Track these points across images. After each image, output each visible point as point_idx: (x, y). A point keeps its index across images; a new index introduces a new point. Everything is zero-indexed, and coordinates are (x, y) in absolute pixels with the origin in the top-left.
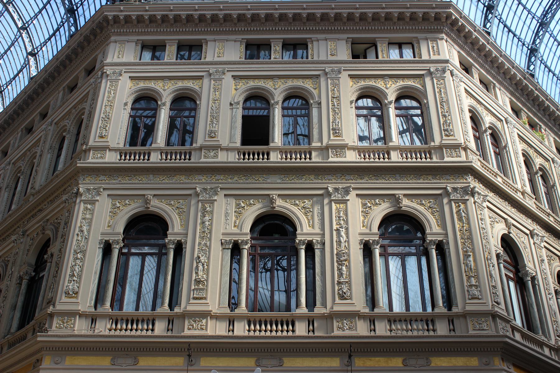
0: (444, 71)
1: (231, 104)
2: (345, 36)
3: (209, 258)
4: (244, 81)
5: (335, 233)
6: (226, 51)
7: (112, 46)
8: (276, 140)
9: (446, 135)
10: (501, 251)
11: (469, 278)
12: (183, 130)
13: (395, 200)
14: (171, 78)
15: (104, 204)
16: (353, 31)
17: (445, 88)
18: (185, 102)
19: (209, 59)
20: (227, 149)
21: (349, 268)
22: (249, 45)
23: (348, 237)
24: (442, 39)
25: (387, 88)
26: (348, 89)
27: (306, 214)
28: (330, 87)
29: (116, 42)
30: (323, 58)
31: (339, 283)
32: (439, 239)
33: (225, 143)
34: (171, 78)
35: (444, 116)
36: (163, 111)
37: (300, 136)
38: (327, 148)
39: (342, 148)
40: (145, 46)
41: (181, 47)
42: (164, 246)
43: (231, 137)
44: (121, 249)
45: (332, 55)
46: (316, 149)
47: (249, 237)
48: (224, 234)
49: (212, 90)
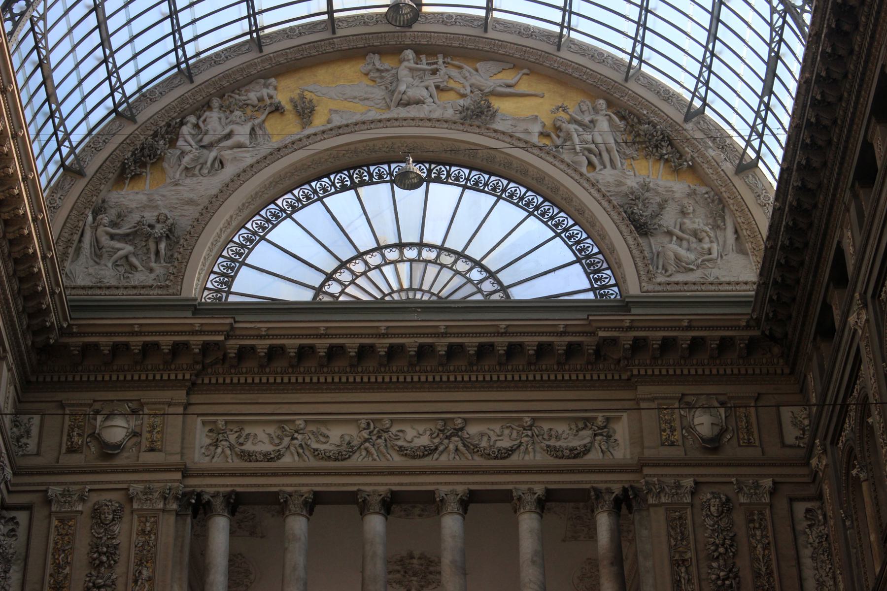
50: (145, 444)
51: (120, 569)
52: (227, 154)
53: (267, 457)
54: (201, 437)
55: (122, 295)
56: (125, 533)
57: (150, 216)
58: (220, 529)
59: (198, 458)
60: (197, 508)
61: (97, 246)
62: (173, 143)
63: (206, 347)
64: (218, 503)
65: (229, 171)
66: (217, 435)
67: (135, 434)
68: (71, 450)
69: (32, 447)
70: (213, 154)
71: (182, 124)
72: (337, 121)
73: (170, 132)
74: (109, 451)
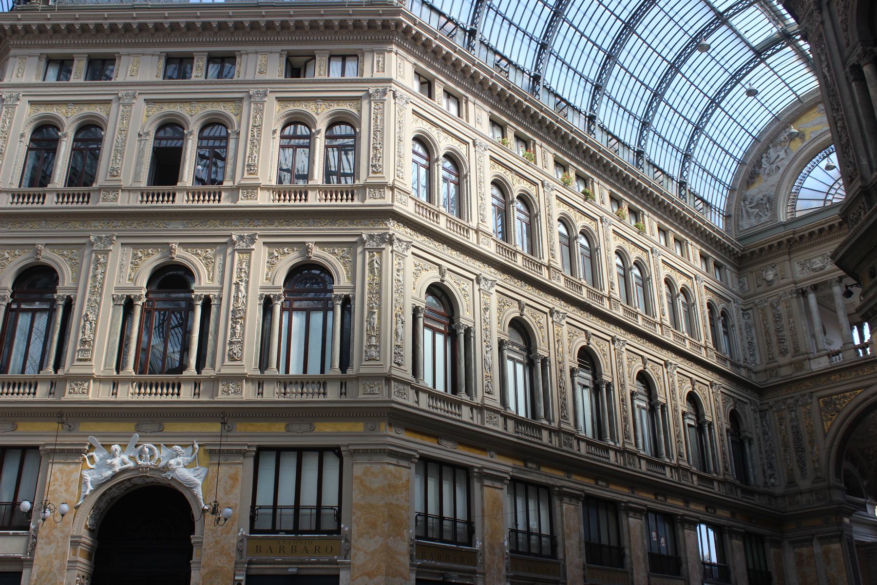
0: (384, 93)
1: (140, 135)
2: (279, 48)
3: (97, 316)
5: (234, 287)
7: (11, 59)
9: (374, 172)
11: (370, 337)
13: (304, 248)
14: (76, 103)
16: (289, 42)
17: (383, 114)
18: (90, 134)
19: (120, 79)
20: (129, 190)
21: (243, 326)
22: (170, 59)
23: (247, 292)
24: (391, 51)
25: (317, 114)
26: (274, 114)
27: (207, 265)
28: (252, 112)
29: (15, 57)
30: (249, 77)
31: (231, 343)
32: (345, 293)
33: (126, 181)
34: (76, 103)
35: (376, 148)
36: (64, 143)
38: (238, 188)
40: (50, 61)
41: (92, 61)
42: (53, 302)
43: (137, 175)
44: (9, 305)
45: (260, 73)
46: (227, 189)
47: (144, 292)
48: (116, 289)
49: (120, 117)
50: (780, 277)
51: (783, 321)
52: (779, 164)
53: (821, 269)
54: (798, 268)
55: (760, 228)
56: (782, 308)
57: (760, 196)
58: (812, 298)
59: (799, 276)
60: (803, 293)
61: (747, 212)
62: (760, 167)
63: (789, 240)
64: (809, 290)
65: (782, 170)
66: (803, 265)
67: (776, 275)
68: (759, 286)
69: (747, 289)
70: (774, 166)
71: (762, 158)
72: (813, 136)
73: (758, 164)
74: (770, 283)
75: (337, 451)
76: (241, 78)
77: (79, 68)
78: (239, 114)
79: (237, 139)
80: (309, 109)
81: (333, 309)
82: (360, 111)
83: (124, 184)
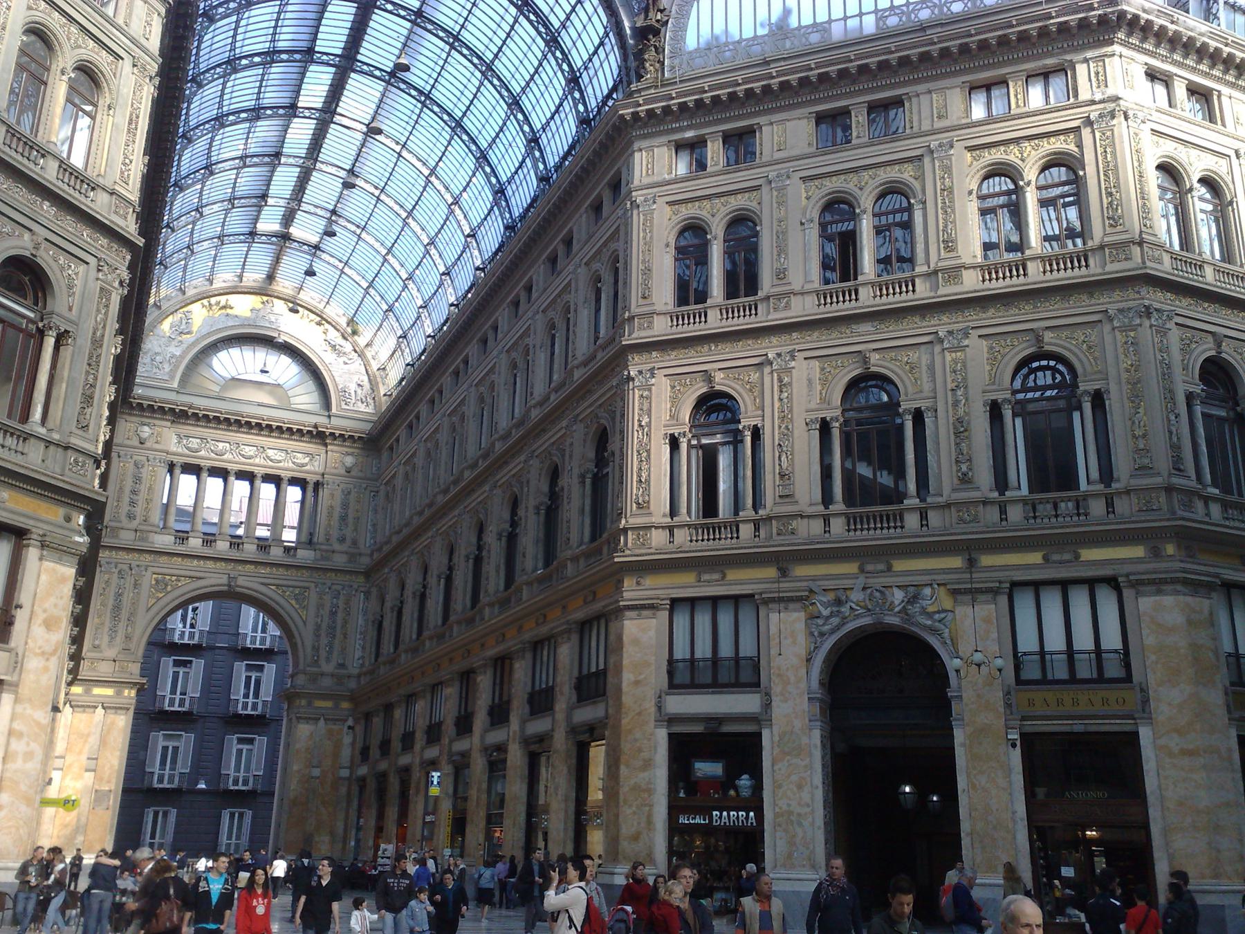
1: (802, 224)
4: (817, 182)
5: (950, 393)
6: (787, 134)
8: (866, 270)
9: (1111, 226)
10: (1198, 388)
12: (743, 280)
15: (662, 386)
17: (1113, 145)
18: (743, 229)
22: (820, 119)
28: (937, 172)
30: (926, 126)
36: (715, 247)
37: (897, 260)
38: (936, 272)
39: (954, 273)
40: (679, 147)
42: (737, 433)
44: (689, 441)
45: (939, 117)
47: (838, 412)
49: (775, 205)
75: (1112, 582)
76: (915, 129)
77: (715, 152)
78: (921, 178)
79: (924, 209)
80: (1012, 155)
81: (1079, 408)
82: (1080, 146)
83: (796, 286)
